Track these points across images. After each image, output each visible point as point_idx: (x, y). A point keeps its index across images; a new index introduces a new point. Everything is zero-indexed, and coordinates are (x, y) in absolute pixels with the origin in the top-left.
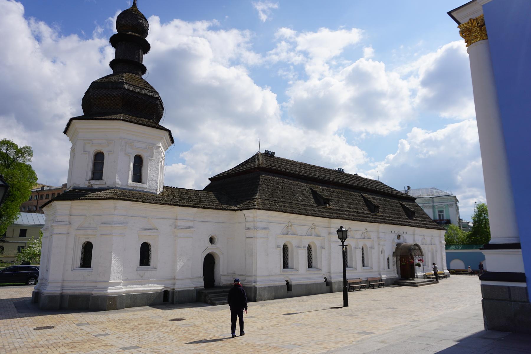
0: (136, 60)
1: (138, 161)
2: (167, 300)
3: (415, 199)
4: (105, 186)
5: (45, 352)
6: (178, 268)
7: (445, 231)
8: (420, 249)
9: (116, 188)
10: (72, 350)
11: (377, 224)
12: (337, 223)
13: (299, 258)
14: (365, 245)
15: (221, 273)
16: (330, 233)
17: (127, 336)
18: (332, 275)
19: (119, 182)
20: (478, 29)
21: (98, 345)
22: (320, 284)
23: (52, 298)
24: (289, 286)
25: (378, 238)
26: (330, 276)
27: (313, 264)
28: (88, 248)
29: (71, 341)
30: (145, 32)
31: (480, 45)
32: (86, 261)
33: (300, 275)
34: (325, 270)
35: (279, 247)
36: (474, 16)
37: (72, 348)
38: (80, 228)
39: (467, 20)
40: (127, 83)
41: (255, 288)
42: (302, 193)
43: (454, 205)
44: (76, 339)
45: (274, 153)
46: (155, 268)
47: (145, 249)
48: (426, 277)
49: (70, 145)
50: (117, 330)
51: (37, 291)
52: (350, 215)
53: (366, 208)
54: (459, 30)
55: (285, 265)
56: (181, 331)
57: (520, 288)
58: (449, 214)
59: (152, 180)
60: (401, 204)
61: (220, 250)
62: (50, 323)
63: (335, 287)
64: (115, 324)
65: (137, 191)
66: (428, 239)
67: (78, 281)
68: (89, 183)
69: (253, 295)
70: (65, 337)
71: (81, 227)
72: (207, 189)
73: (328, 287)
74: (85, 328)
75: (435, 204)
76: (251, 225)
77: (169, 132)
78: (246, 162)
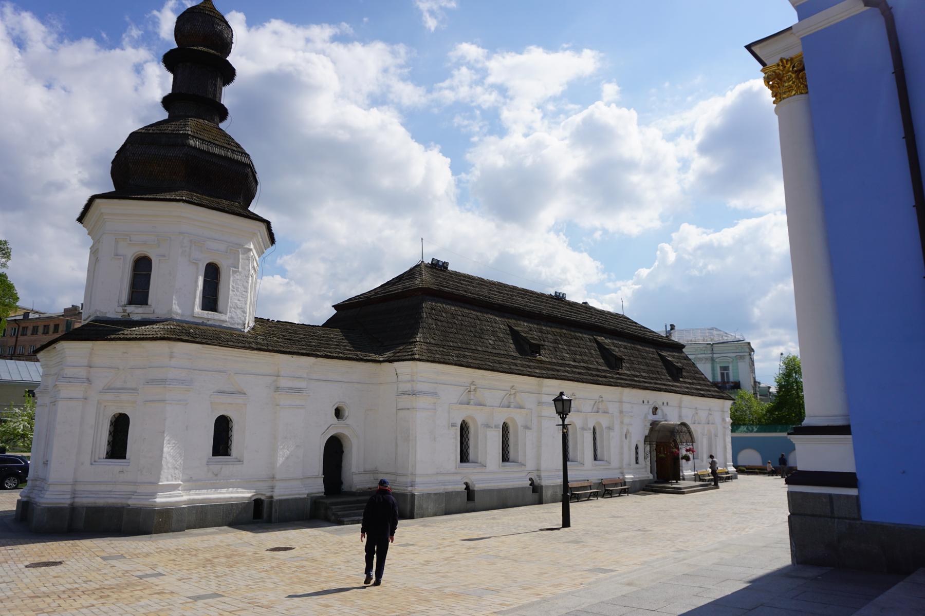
0: (210, 96)
1: (213, 274)
2: (259, 515)
3: (683, 346)
4: (153, 317)
5: (55, 604)
6: (280, 460)
7: (731, 402)
8: (690, 432)
9: (172, 319)
10: (102, 601)
11: (620, 388)
12: (553, 387)
13: (488, 445)
14: (599, 424)
15: (354, 470)
16: (540, 403)
17: (195, 576)
18: (543, 474)
19: (177, 310)
20: (793, 76)
21: (147, 592)
22: (523, 489)
23: (55, 512)
24: (470, 493)
25: (621, 412)
26: (539, 476)
27: (511, 455)
28: (120, 427)
29: (98, 586)
30: (226, 45)
31: (796, 102)
32: (117, 446)
33: (489, 473)
34: (530, 465)
35: (453, 425)
36: (787, 55)
37: (101, 597)
38: (108, 389)
39: (776, 60)
40: (193, 137)
41: (413, 495)
42: (494, 333)
43: (747, 358)
44: (106, 582)
45: (447, 264)
46: (240, 461)
47: (223, 427)
48: (698, 477)
49: (91, 242)
50: (177, 568)
51: (25, 499)
52: (575, 373)
54: (763, 75)
55: (464, 457)
56: (289, 568)
57: (848, 497)
58: (738, 372)
59: (236, 307)
60: (659, 355)
61: (353, 431)
62: (55, 556)
63: (547, 494)
64: (173, 557)
65: (210, 326)
66: (703, 415)
67: (105, 483)
68: (124, 311)
69: (409, 507)
70: (85, 579)
71: (109, 389)
72: (330, 323)
73: (535, 494)
74: (120, 565)
75: (715, 356)
76: (407, 387)
77: (268, 224)
78: (399, 279)
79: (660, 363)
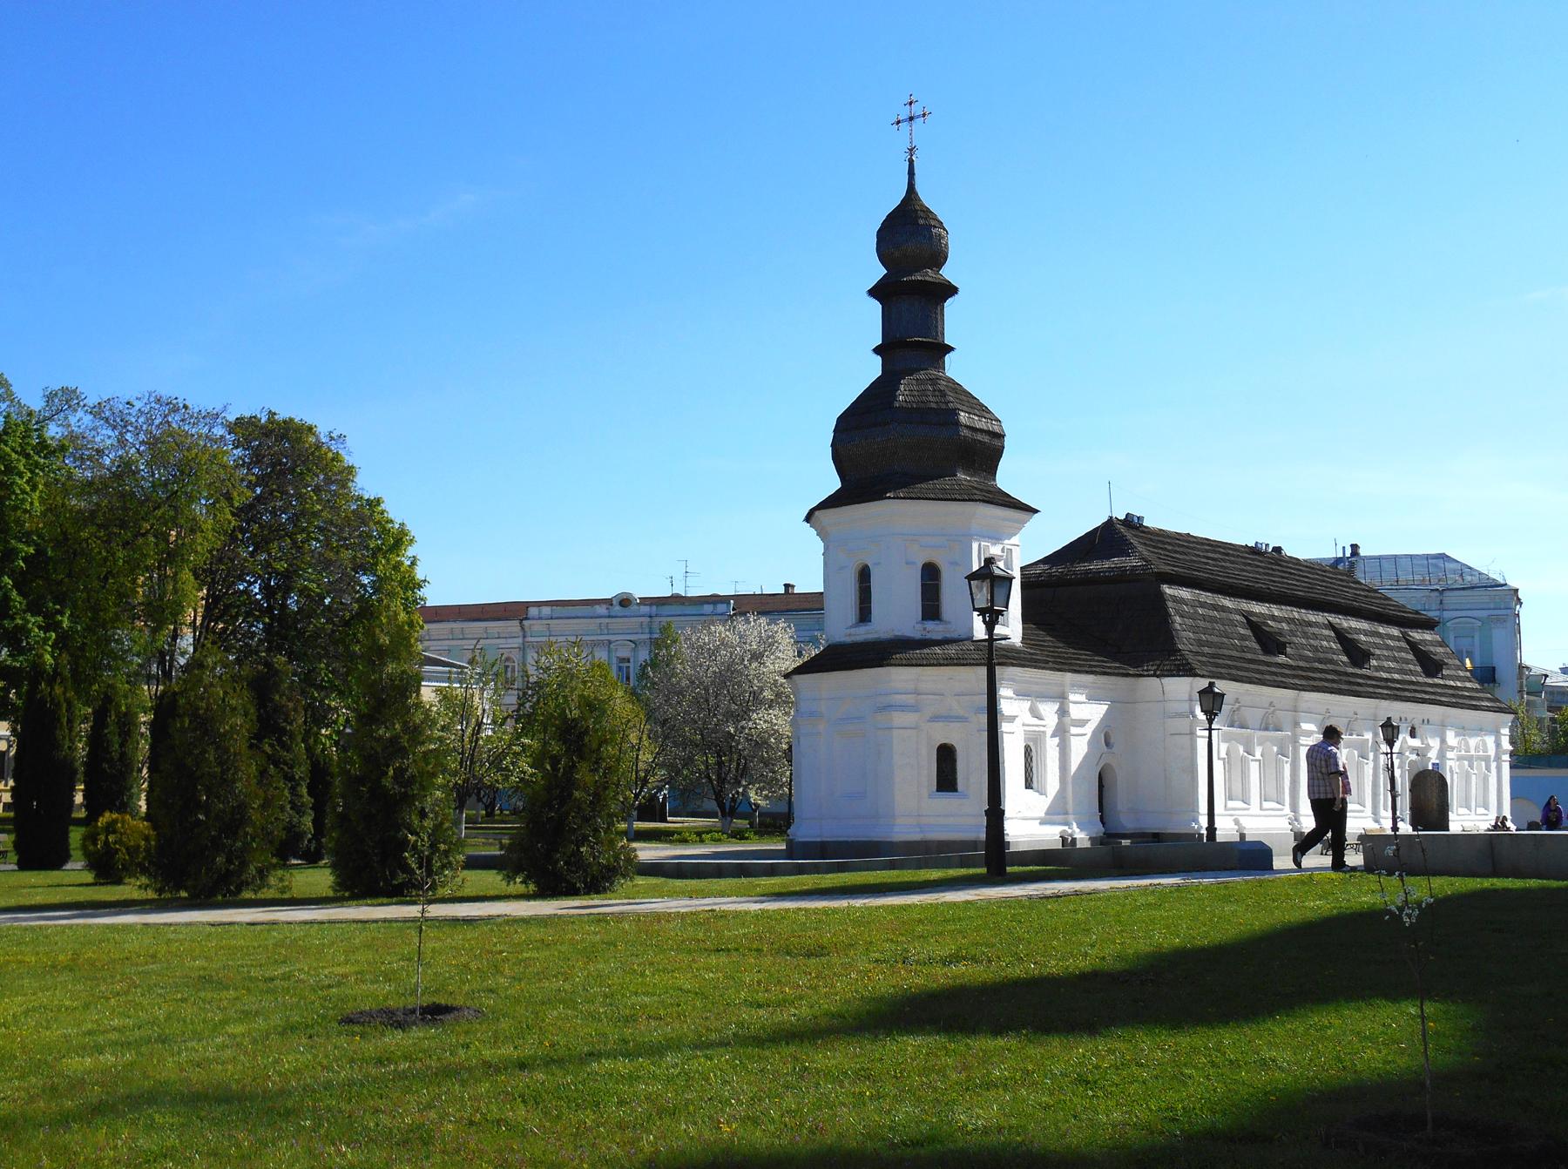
4: (955, 635)
7: (1511, 717)
15: (1119, 807)
28: (946, 755)
30: (938, 257)
32: (946, 780)
53: (1345, 659)
75: (1447, 615)
79: (1411, 657)
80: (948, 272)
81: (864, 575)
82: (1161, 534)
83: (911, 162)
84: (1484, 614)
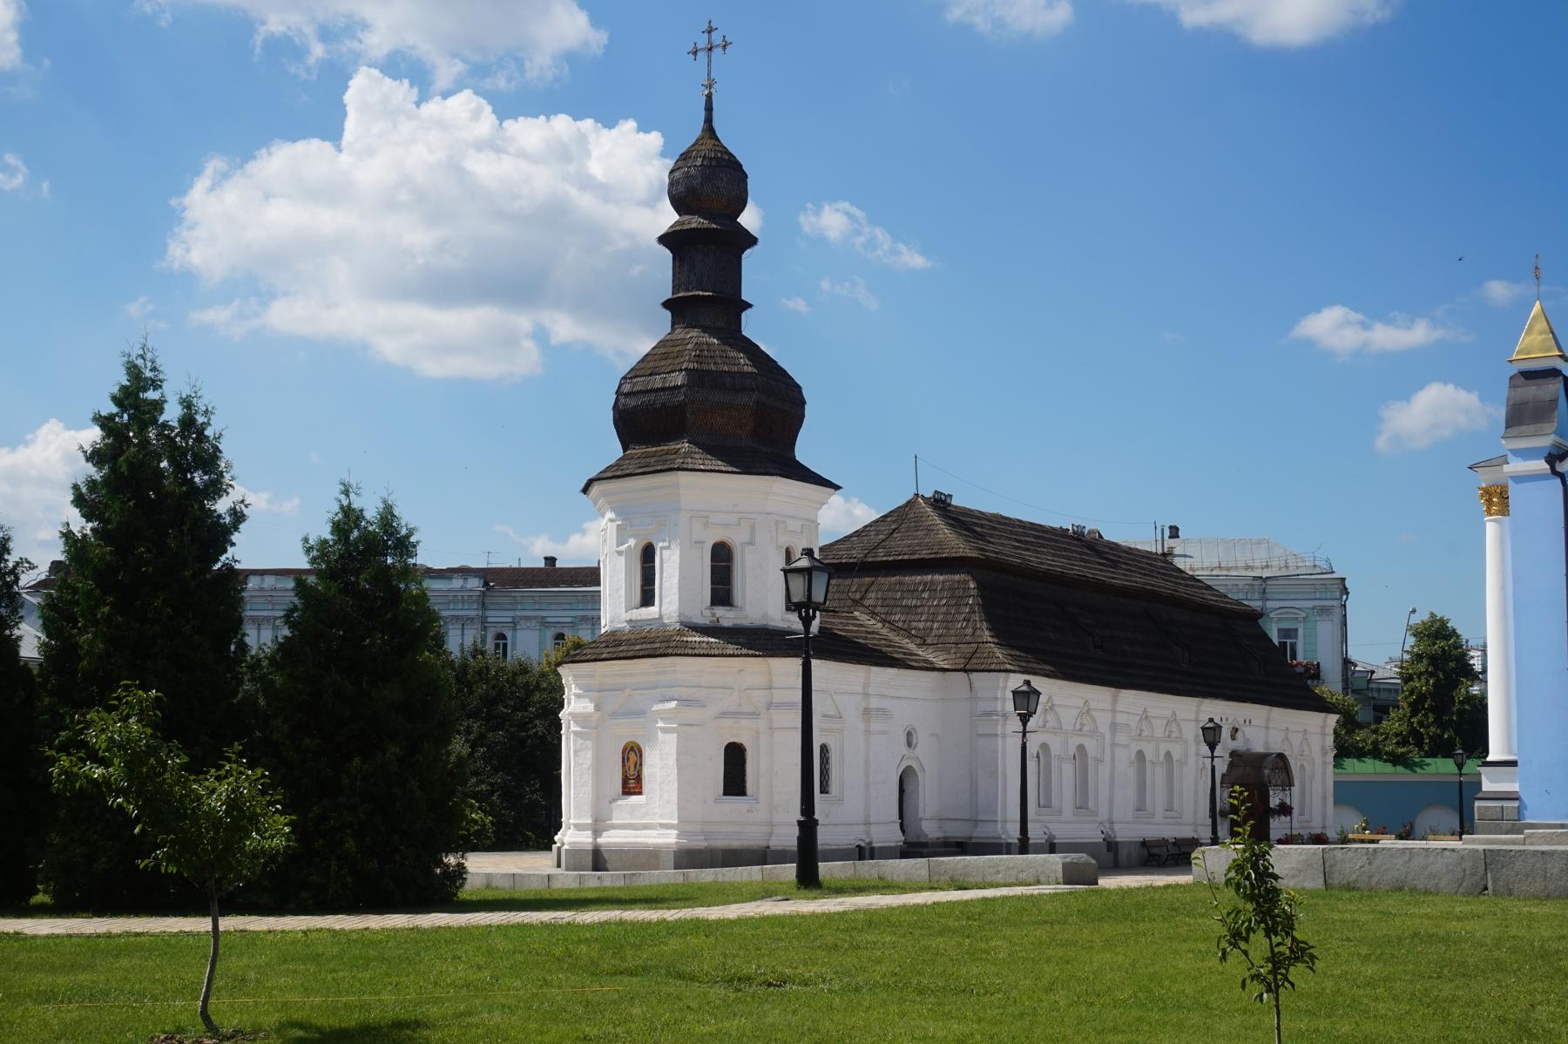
18: (1116, 827)
28: (735, 757)
32: (735, 783)
34: (1103, 815)
58: (1316, 647)
63: (1123, 853)
75: (1270, 604)
80: (749, 219)
81: (648, 554)
82: (1114, 547)
83: (709, 97)
84: (1310, 604)
